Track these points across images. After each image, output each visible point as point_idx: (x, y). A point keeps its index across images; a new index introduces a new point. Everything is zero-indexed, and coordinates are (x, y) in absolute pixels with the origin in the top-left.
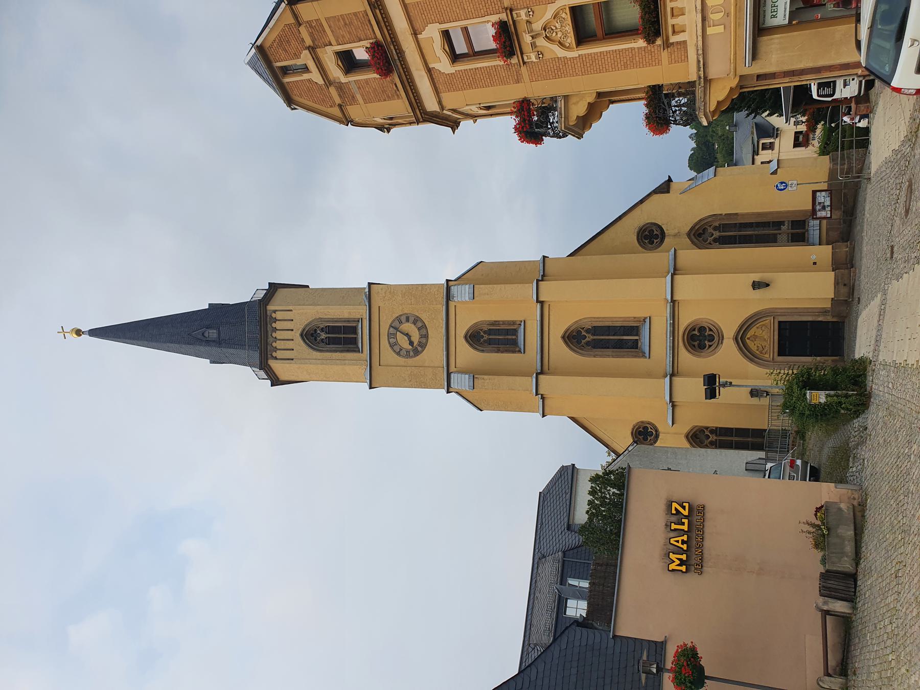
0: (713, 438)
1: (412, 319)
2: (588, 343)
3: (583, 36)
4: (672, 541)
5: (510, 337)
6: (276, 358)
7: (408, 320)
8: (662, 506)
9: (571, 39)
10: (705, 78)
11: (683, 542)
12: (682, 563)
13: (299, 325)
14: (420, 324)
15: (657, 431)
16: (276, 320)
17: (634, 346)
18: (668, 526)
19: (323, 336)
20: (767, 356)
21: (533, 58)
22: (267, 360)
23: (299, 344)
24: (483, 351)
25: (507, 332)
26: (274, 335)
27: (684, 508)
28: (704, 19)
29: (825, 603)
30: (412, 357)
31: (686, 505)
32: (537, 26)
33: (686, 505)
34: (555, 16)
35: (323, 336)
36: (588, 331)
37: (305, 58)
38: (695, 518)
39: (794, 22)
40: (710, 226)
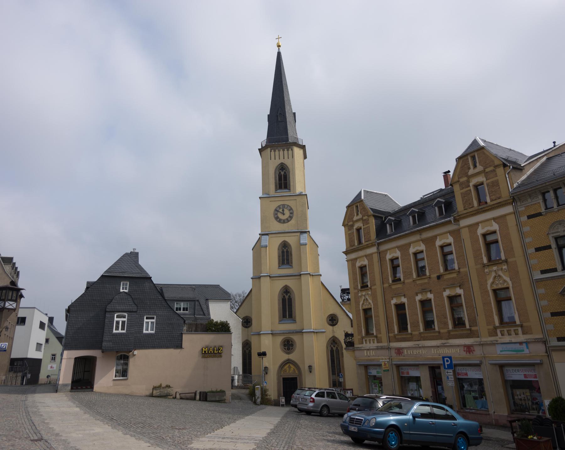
0: (247, 352)
1: (291, 215)
2: (284, 296)
4: (211, 348)
5: (286, 261)
6: (271, 151)
7: (291, 213)
8: (221, 344)
10: (355, 350)
11: (211, 352)
12: (205, 352)
13: (287, 162)
14: (289, 219)
15: (249, 327)
16: (288, 150)
17: (284, 316)
18: (215, 347)
19: (282, 173)
20: (282, 373)
21: (360, 295)
22: (270, 147)
23: (278, 162)
24: (279, 249)
25: (288, 260)
26: (281, 150)
27: (221, 351)
28: (368, 349)
29: (198, 393)
30: (274, 216)
31: (222, 352)
32: (367, 297)
33: (222, 352)
34: (370, 303)
35: (282, 173)
36: (289, 296)
37: (360, 216)
38: (218, 354)
39: (368, 376)
40: (338, 346)
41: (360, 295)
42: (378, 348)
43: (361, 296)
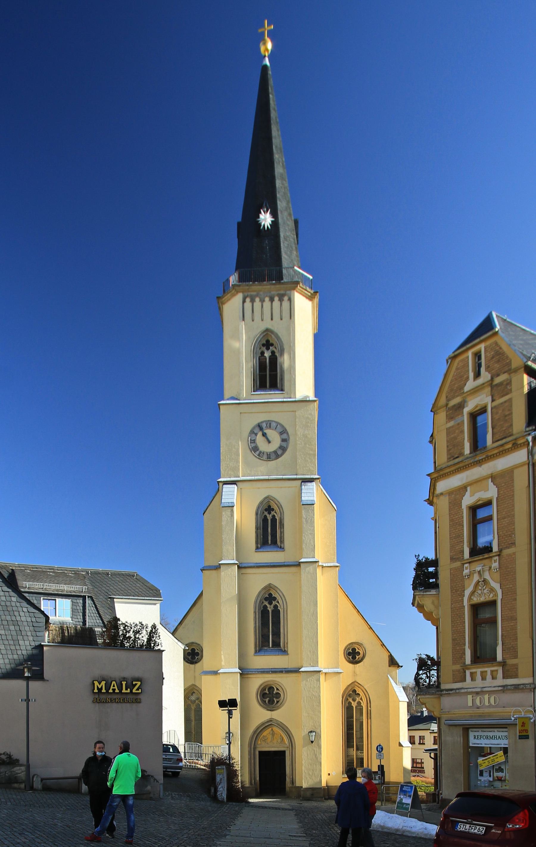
3: (476, 608)
9: (476, 600)
28: (477, 693)
32: (487, 576)
34: (492, 590)
41: (466, 572)
42: (505, 688)
43: (469, 576)
